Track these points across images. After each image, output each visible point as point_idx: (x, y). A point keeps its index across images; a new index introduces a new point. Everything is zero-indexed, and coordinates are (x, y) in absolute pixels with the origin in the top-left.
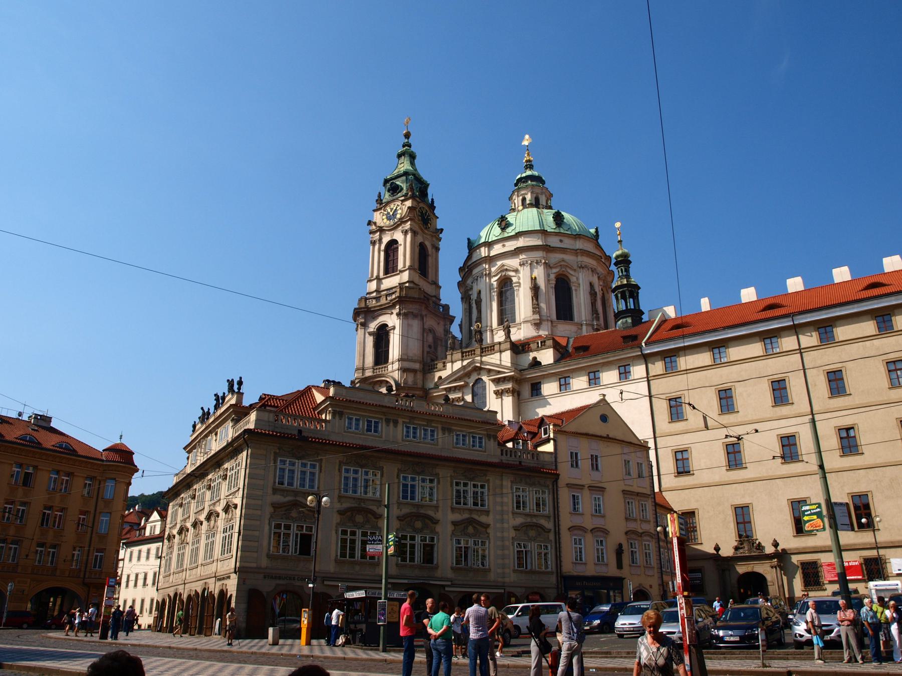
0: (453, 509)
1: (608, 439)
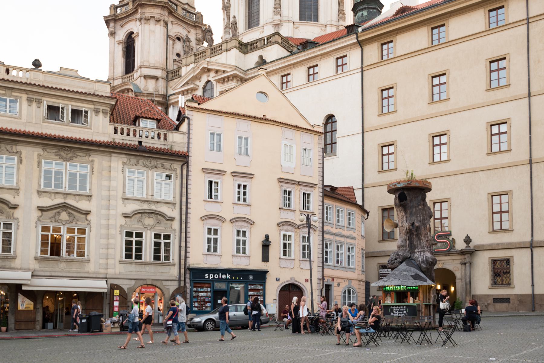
0: (39, 192)
1: (264, 120)
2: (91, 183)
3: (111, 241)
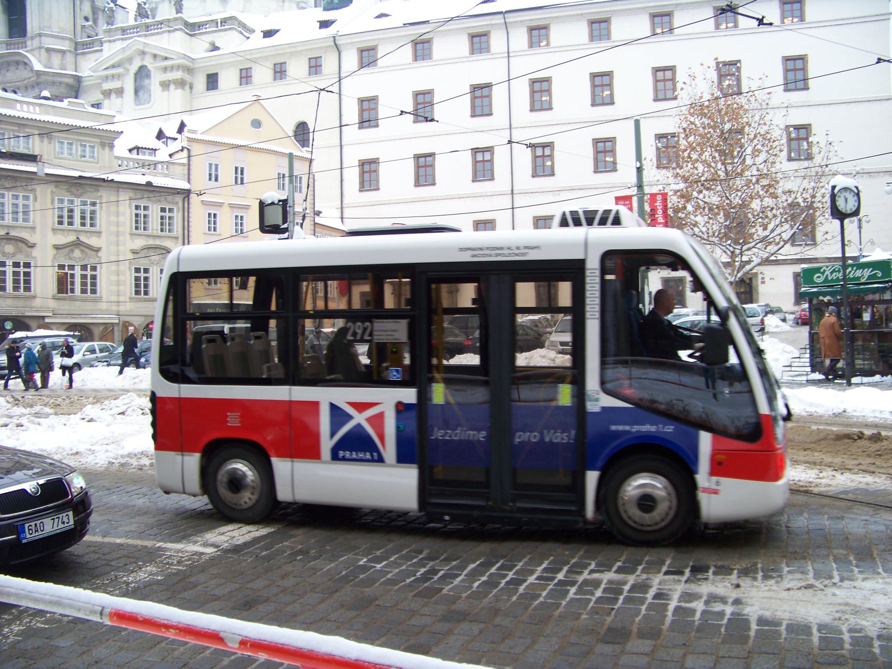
0: (54, 230)
2: (100, 218)
3: (122, 278)
